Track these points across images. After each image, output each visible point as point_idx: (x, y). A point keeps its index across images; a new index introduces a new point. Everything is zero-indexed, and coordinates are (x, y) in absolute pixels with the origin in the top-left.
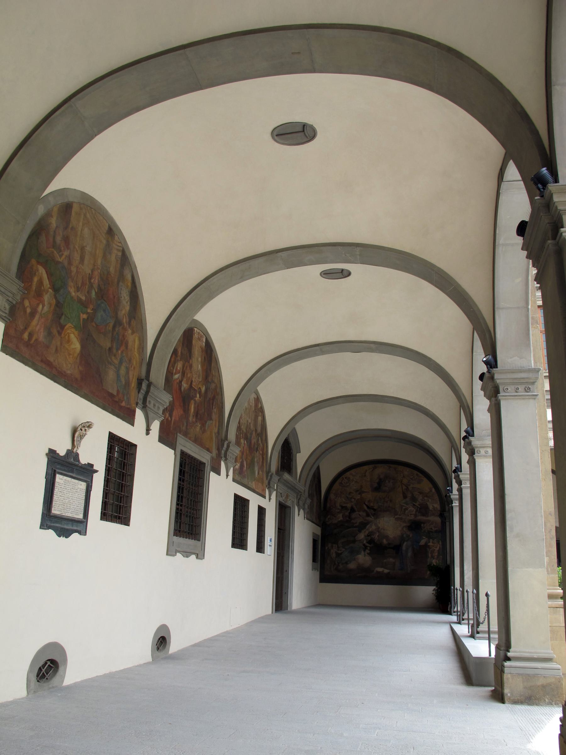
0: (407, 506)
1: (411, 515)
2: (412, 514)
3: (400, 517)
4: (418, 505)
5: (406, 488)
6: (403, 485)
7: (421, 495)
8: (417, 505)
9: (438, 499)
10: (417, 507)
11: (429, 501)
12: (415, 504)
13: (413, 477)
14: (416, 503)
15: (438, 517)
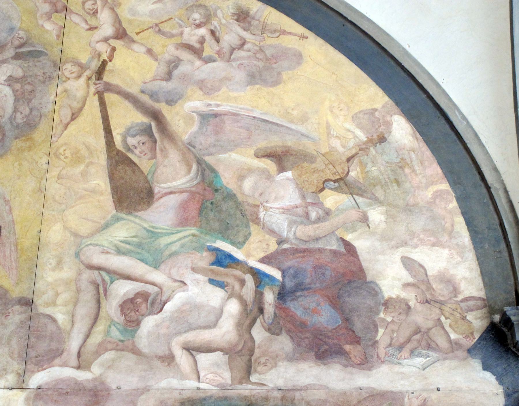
0: (157, 277)
1: (203, 359)
2: (209, 349)
3: (83, 376)
4: (266, 260)
5: (141, 119)
6: (109, 97)
7: (289, 174)
8: (253, 263)
9: (454, 204)
10: (255, 273)
11: (365, 219)
12: (239, 254)
13: (203, 31)
14: (239, 245)
15: (476, 364)
